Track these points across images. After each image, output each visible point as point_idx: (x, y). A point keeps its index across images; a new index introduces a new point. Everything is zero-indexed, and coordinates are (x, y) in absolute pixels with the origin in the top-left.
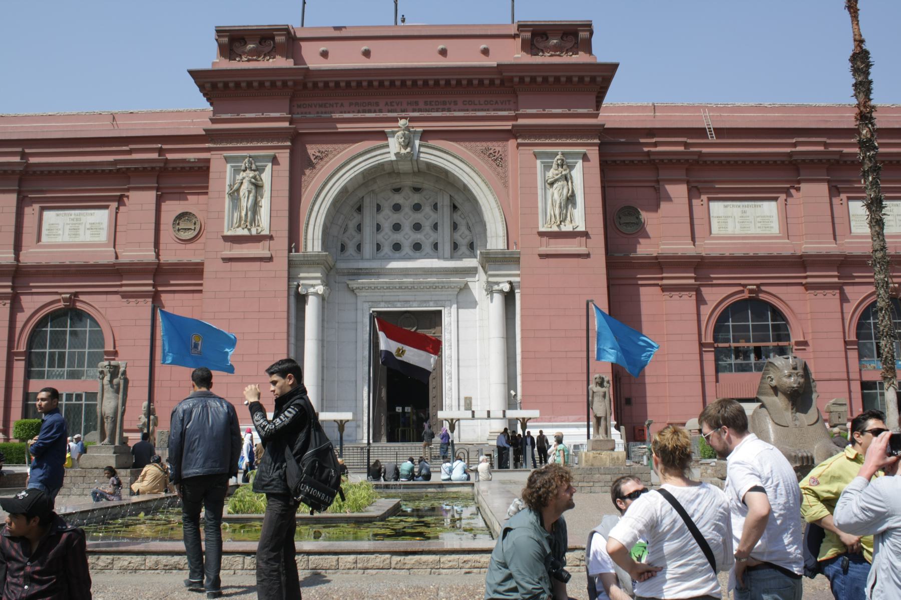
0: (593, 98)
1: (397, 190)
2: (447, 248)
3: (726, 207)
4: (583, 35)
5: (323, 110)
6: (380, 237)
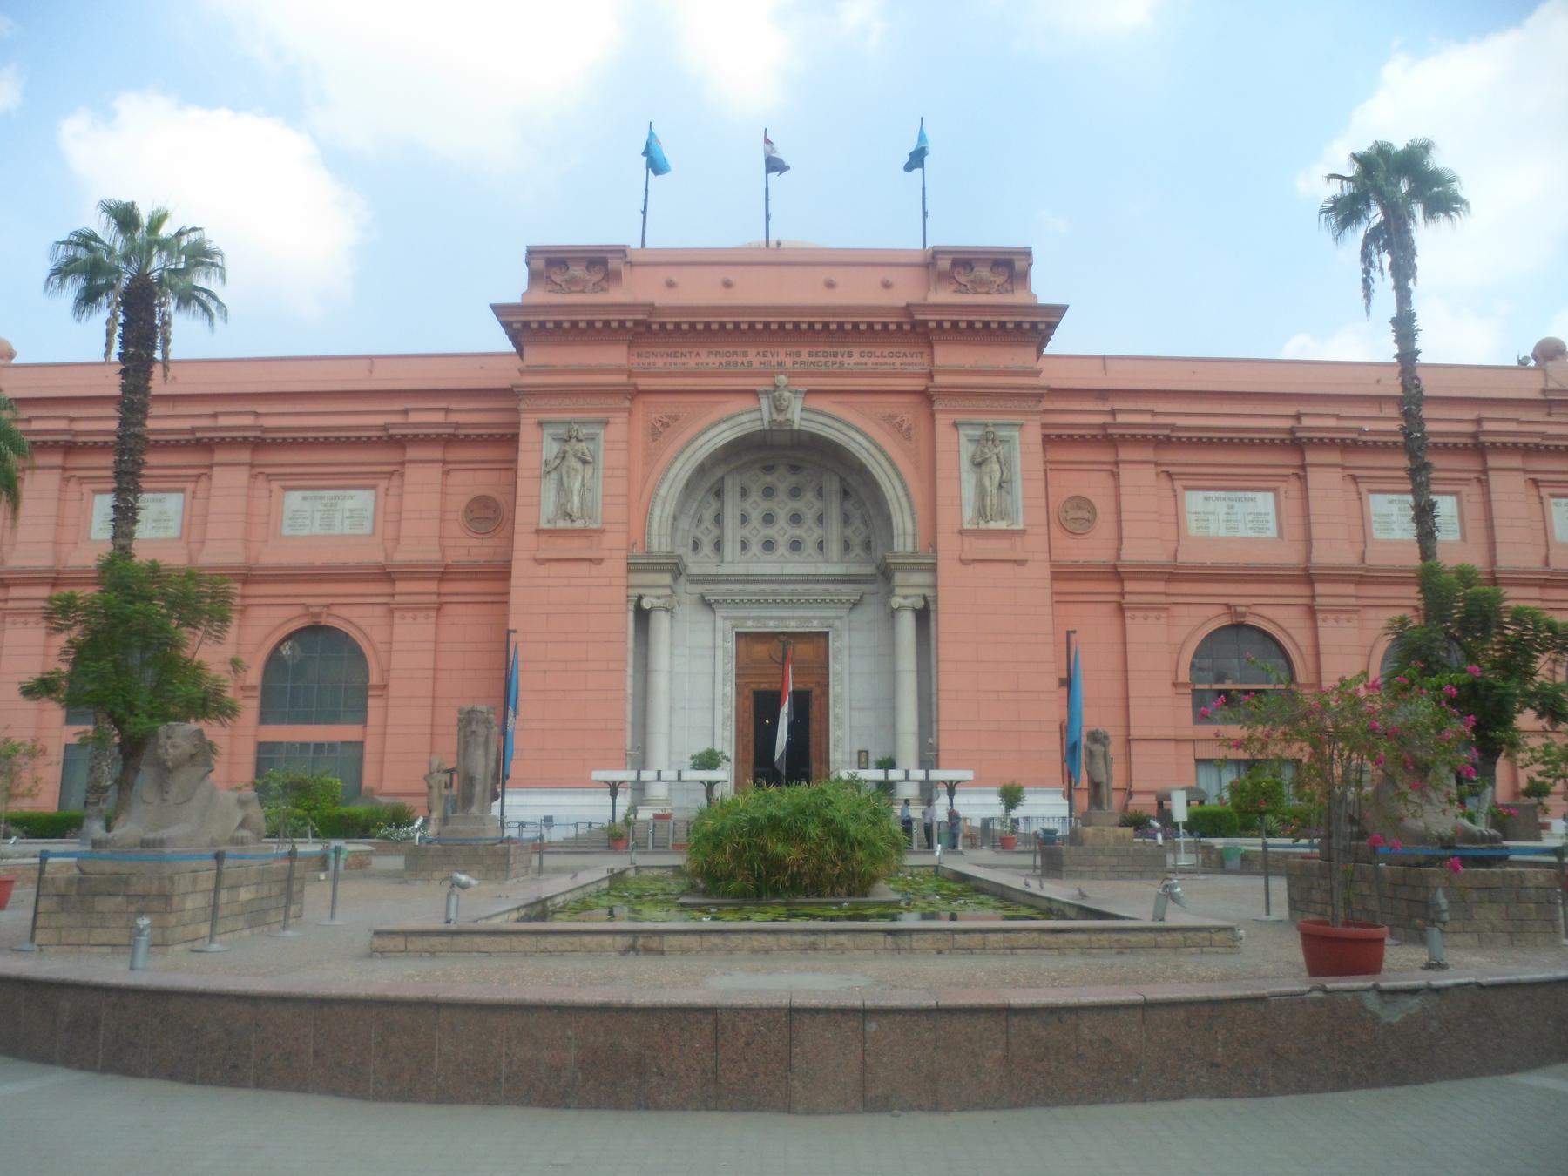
0: (1033, 350)
1: (768, 469)
2: (835, 548)
3: (1206, 499)
5: (673, 360)
6: (746, 532)
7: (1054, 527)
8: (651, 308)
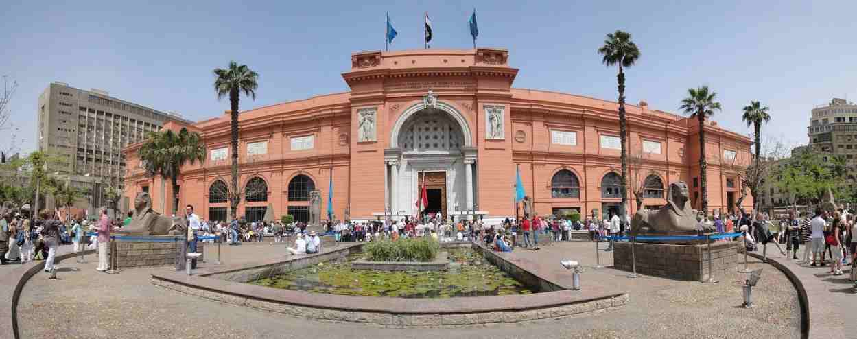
1: (427, 122)
4: (504, 55)
7: (513, 140)
8: (389, 70)
